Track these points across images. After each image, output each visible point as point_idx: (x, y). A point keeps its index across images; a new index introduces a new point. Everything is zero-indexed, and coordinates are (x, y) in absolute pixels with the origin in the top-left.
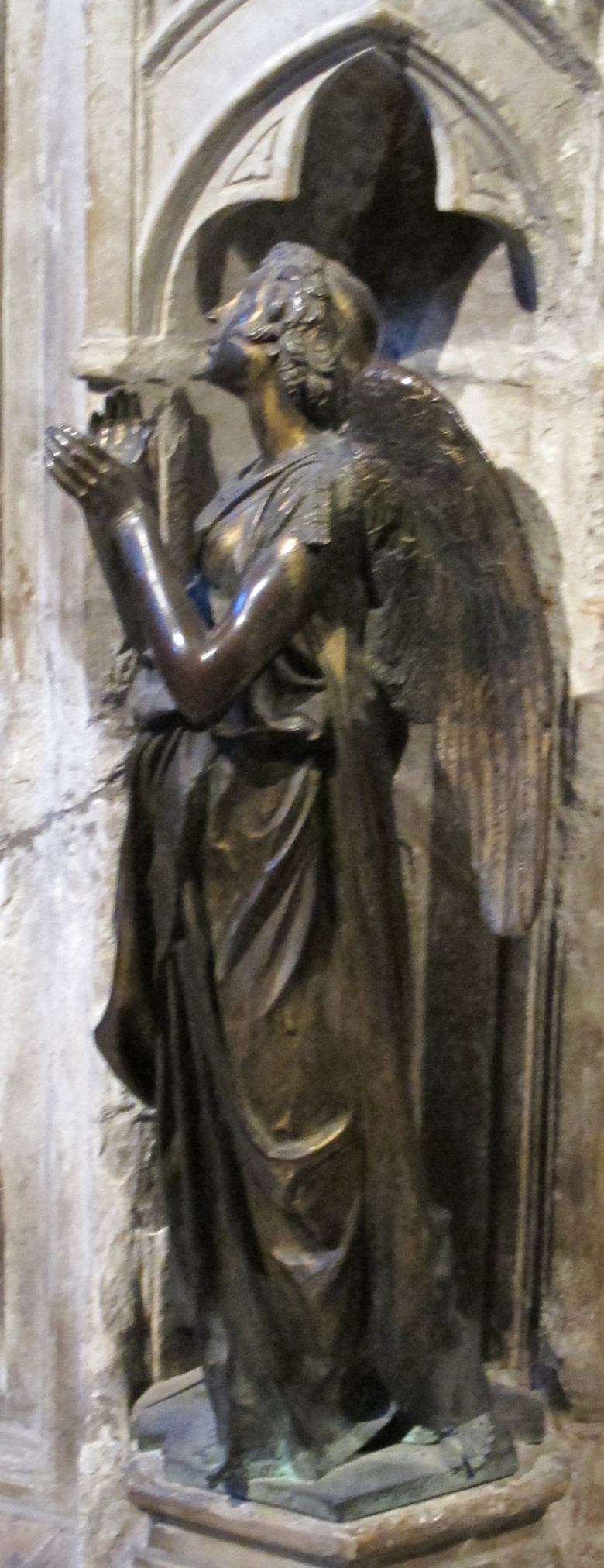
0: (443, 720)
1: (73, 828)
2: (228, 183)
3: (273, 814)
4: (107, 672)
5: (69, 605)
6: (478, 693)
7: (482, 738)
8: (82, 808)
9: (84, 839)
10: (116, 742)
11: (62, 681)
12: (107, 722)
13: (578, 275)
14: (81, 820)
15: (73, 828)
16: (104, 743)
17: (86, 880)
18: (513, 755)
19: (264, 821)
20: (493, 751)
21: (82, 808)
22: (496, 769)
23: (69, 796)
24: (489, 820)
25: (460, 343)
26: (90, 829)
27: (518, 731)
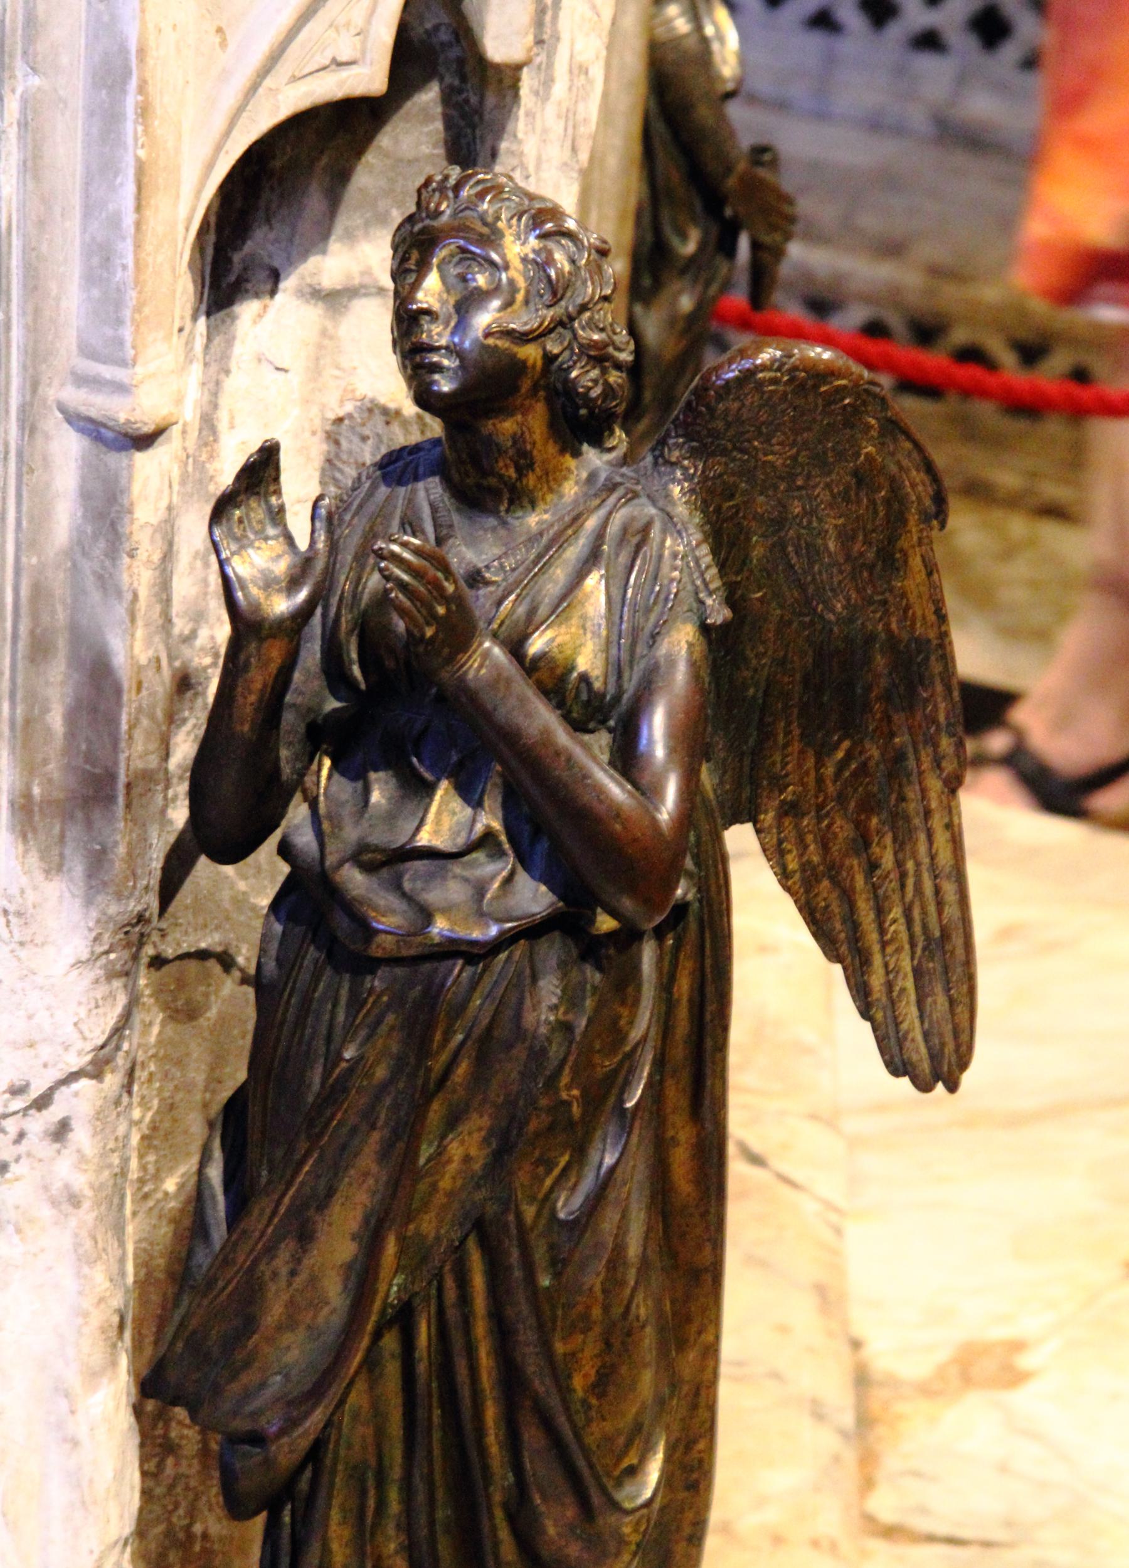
0: (768, 818)
1: (21, 1135)
2: (294, 79)
3: (631, 1023)
4: (145, 882)
5: (36, 791)
6: (829, 770)
7: (843, 829)
8: (42, 1102)
9: (47, 1149)
10: (117, 984)
11: (19, 914)
12: (112, 956)
13: (551, 109)
14: (38, 1124)
15: (21, 1135)
16: (102, 990)
17: (46, 1212)
18: (902, 843)
19: (619, 1036)
20: (863, 841)
21: (42, 1102)
22: (873, 866)
23: (16, 1091)
24: (873, 937)
25: (350, 237)
26: (61, 1131)
27: (913, 807)
